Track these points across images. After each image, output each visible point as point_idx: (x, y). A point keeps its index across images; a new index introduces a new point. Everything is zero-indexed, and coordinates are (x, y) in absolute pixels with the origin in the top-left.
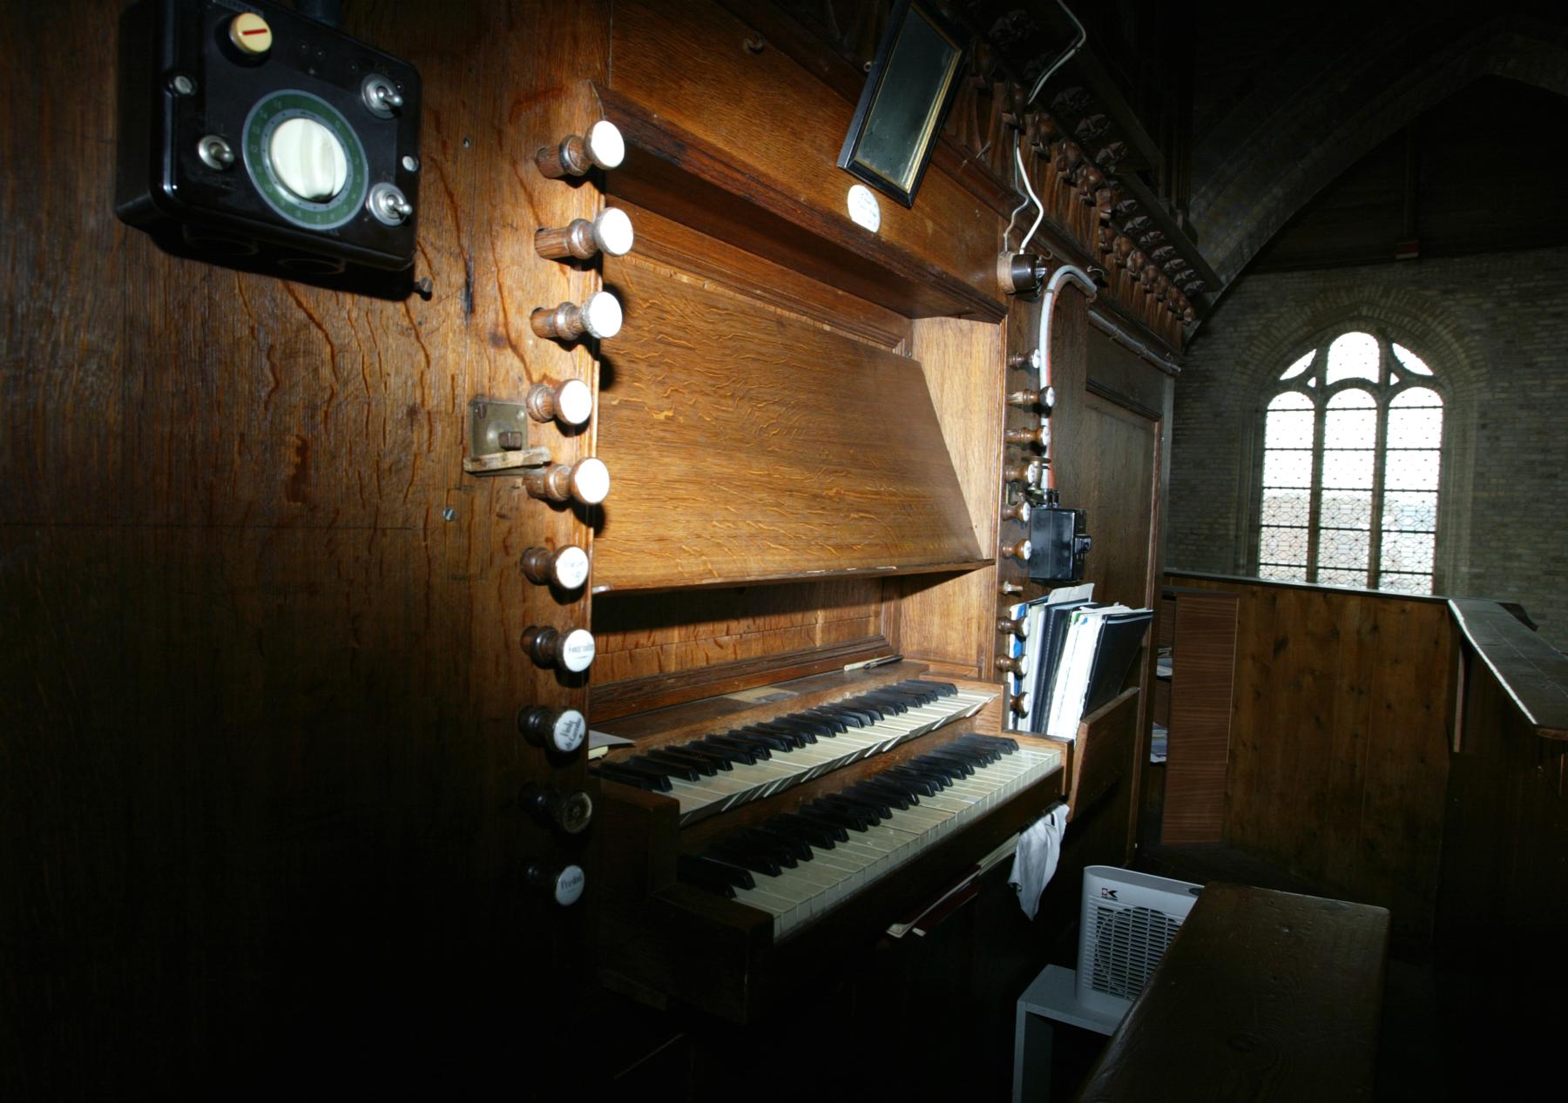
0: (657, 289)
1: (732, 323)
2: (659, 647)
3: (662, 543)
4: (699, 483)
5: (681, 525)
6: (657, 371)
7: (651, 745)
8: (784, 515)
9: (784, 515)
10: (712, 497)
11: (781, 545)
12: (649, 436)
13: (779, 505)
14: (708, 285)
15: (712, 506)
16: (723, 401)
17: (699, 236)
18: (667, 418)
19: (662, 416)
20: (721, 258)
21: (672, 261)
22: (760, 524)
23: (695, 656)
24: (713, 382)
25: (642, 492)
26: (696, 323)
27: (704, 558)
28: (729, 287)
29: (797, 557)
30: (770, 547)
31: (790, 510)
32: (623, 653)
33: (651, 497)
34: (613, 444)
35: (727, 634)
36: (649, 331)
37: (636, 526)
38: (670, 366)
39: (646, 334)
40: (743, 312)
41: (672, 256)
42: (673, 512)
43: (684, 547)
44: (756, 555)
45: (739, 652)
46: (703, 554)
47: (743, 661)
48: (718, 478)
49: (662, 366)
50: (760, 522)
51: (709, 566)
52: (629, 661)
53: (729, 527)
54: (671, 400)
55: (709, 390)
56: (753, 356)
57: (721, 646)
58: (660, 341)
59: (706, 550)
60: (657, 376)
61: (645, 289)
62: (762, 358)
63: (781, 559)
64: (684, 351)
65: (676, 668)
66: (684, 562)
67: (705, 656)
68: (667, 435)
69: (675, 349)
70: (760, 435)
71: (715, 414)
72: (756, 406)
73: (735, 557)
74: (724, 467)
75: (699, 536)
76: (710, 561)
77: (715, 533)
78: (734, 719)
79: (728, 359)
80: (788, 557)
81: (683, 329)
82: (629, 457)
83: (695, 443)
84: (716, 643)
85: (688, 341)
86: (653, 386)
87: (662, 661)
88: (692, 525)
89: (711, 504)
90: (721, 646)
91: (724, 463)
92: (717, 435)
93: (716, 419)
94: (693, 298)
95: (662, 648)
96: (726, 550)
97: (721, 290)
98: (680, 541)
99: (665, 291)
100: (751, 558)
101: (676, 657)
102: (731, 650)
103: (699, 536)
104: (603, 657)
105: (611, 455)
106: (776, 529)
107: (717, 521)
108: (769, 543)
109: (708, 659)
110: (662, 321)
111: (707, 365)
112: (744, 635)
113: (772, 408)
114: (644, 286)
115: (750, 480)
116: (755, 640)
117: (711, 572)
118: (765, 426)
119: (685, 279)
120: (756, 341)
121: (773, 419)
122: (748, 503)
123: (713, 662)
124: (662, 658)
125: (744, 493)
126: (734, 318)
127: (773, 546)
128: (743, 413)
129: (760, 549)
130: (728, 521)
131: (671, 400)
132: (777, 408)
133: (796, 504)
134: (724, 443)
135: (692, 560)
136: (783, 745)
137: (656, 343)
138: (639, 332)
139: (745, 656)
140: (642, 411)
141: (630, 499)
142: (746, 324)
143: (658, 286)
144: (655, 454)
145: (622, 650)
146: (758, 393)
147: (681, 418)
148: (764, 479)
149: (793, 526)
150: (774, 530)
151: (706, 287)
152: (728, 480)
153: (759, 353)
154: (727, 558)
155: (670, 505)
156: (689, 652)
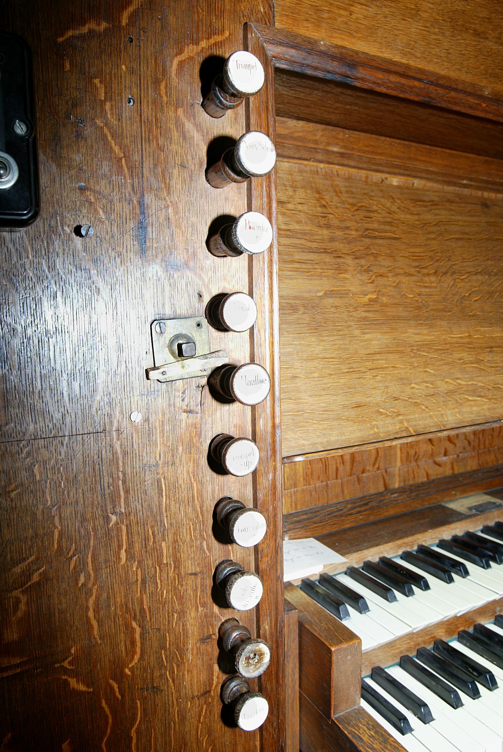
0: (365, 194)
1: (437, 212)
2: (384, 471)
3: (359, 409)
4: (400, 352)
5: (379, 391)
6: (363, 262)
7: (367, 557)
8: (484, 370)
9: (484, 370)
10: (413, 363)
11: (479, 396)
12: (351, 318)
13: (479, 361)
14: (417, 183)
15: (410, 371)
16: (426, 279)
17: (406, 145)
18: (370, 300)
19: (366, 299)
20: (428, 159)
21: (381, 168)
22: (458, 381)
23: (416, 475)
24: (416, 264)
25: (343, 367)
26: (402, 216)
27: (400, 417)
28: (437, 181)
29: (495, 406)
30: (468, 400)
31: (489, 365)
32: (352, 478)
33: (351, 370)
34: (317, 329)
35: (445, 455)
36: (357, 230)
37: (334, 398)
38: (375, 256)
39: (353, 233)
40: (449, 201)
41: (381, 165)
42: (372, 382)
43: (381, 410)
44: (454, 409)
45: (456, 468)
46: (400, 415)
47: (461, 475)
48: (419, 345)
49: (368, 257)
50: (458, 379)
51: (406, 424)
52: (357, 483)
53: (427, 387)
54: (375, 284)
55: (413, 271)
56: (457, 236)
57: (439, 465)
58: (366, 236)
59: (402, 411)
60: (362, 266)
61: (354, 196)
62: (466, 236)
63: (478, 409)
64: (389, 241)
65: (399, 485)
66: (380, 423)
67: (425, 473)
68: (370, 315)
69: (380, 241)
70: (461, 303)
71: (417, 290)
72: (458, 278)
73: (431, 413)
74: (425, 335)
75: (396, 399)
76: (406, 420)
77: (413, 394)
78: (444, 531)
79: (433, 242)
80: (485, 407)
81: (390, 224)
82: (331, 338)
83: (397, 319)
84: (435, 463)
85: (394, 232)
86: (358, 275)
87: (387, 481)
88: (390, 390)
89: (410, 369)
90: (439, 465)
91: (425, 332)
92: (419, 308)
93: (419, 295)
94: (399, 196)
95: (386, 471)
96: (423, 407)
97: (429, 184)
98: (377, 405)
99: (373, 194)
100: (449, 412)
101: (399, 476)
102: (449, 467)
103: (396, 399)
104: (334, 483)
105: (313, 339)
106: (474, 383)
107: (415, 383)
108: (467, 397)
109: (428, 475)
110: (368, 219)
111: (411, 250)
112: (461, 455)
113: (474, 278)
114: (353, 193)
115: (450, 343)
116: (470, 458)
117: (407, 429)
118: (467, 295)
119: (395, 181)
120: (460, 223)
121: (475, 287)
122: (448, 364)
123: (432, 478)
124: (387, 478)
125: (444, 355)
126: (439, 207)
127: (470, 398)
128: (446, 286)
129: (458, 403)
130: (426, 382)
131: (375, 284)
132: (479, 277)
133: (496, 358)
134: (426, 314)
135: (389, 421)
136: (482, 562)
137: (363, 239)
138: (347, 232)
139: (462, 470)
140: (347, 298)
141: (331, 375)
142: (450, 210)
143: (366, 191)
144: (357, 332)
145: (351, 476)
146: (461, 267)
147: (384, 298)
148: (464, 341)
149: (492, 378)
150: (472, 384)
151: (415, 185)
152: (428, 346)
153: (463, 233)
154: (424, 415)
155: (369, 375)
156: (411, 471)
